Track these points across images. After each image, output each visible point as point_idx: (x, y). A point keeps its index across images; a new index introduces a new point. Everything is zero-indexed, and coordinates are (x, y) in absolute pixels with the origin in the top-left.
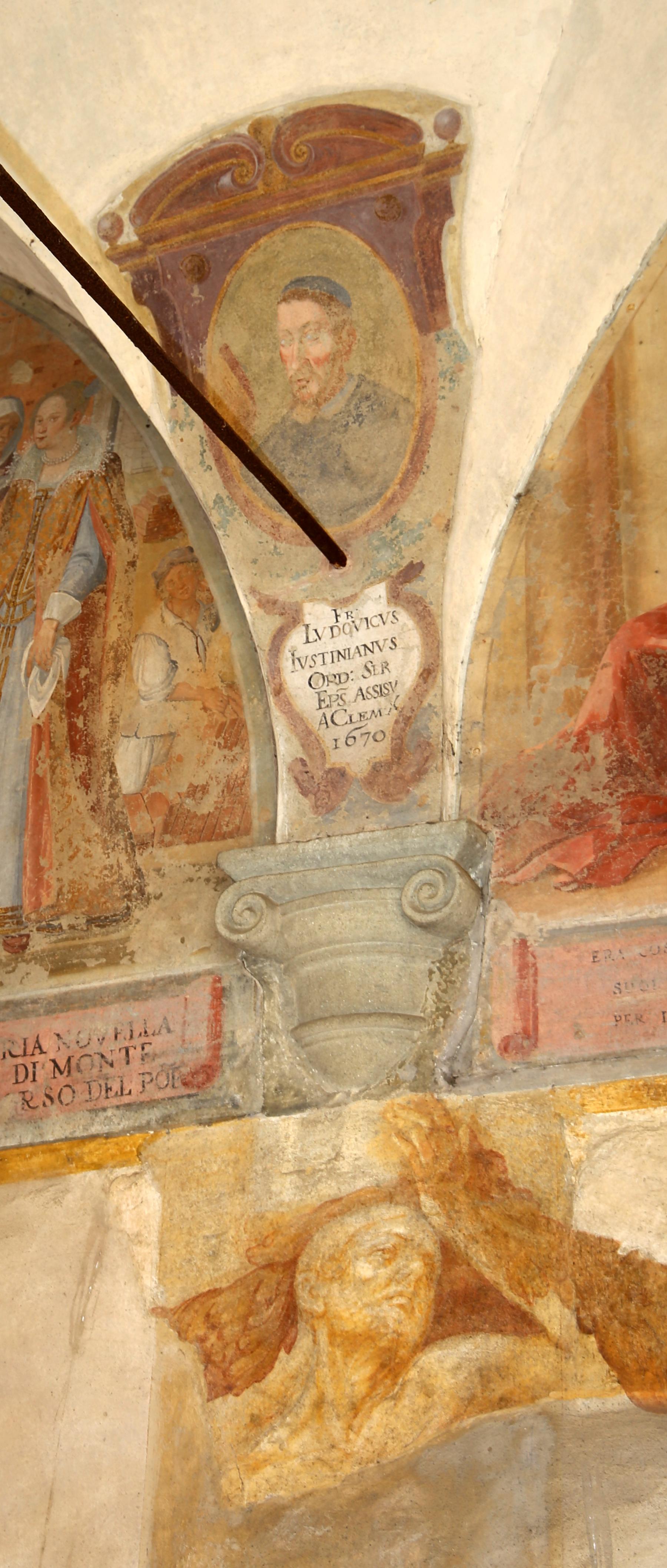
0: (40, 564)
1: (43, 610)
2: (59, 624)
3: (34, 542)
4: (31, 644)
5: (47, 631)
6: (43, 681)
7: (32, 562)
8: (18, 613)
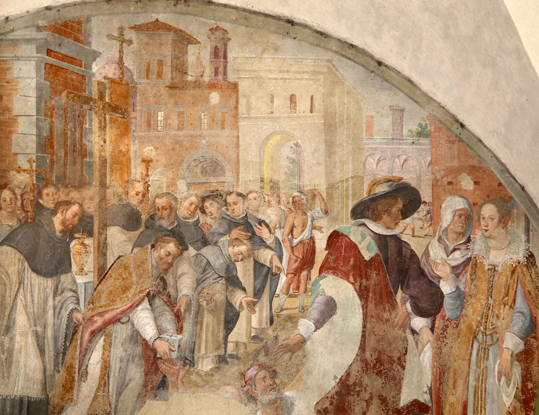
0: (497, 312)
1: (503, 342)
2: (512, 353)
3: (491, 297)
4: (498, 361)
5: (507, 356)
6: (508, 386)
7: (492, 310)
8: (489, 342)
